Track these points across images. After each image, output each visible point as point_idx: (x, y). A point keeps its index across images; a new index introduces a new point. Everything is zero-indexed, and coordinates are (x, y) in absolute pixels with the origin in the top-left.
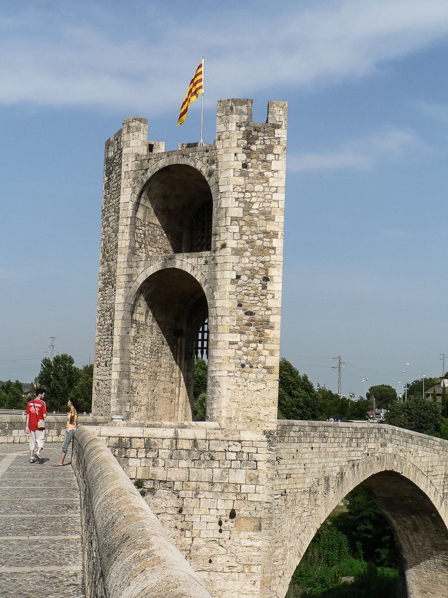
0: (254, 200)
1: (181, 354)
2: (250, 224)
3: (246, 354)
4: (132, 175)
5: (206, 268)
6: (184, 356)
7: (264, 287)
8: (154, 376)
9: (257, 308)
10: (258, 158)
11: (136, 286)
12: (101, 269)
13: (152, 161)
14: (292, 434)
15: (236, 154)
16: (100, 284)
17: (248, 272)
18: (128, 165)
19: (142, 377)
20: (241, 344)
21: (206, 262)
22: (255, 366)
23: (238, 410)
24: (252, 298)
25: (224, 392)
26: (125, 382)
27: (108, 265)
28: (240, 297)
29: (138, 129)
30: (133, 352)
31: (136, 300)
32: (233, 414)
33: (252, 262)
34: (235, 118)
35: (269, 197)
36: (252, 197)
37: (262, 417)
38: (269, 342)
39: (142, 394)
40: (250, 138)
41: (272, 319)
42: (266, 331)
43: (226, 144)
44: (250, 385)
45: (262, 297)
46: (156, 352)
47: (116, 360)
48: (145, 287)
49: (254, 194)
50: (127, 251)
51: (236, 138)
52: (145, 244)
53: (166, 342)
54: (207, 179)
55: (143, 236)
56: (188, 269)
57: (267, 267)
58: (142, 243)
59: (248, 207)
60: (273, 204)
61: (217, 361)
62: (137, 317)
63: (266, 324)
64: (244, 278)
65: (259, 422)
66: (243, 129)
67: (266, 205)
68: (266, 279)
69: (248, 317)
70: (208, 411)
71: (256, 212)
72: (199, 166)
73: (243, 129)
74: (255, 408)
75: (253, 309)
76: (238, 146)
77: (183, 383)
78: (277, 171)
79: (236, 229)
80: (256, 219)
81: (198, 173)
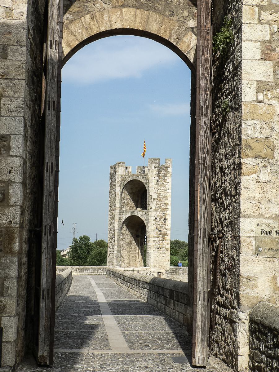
0: (161, 192)
1: (139, 244)
2: (160, 201)
3: (159, 245)
4: (120, 182)
5: (145, 216)
6: (140, 244)
7: (165, 222)
8: (129, 252)
9: (163, 229)
10: (162, 178)
11: (122, 221)
12: (109, 213)
13: (127, 178)
14: (180, 272)
15: (154, 177)
16: (109, 219)
17: (159, 217)
18: (119, 179)
19: (125, 252)
20: (157, 241)
21: (145, 214)
22: (162, 248)
23: (156, 263)
24: (161, 226)
25: (152, 257)
26: (119, 254)
27: (112, 212)
28: (157, 225)
29: (122, 166)
30: (122, 244)
31: (122, 226)
32: (155, 264)
33: (160, 213)
34: (154, 165)
35: (166, 191)
36: (160, 192)
37: (165, 265)
38: (166, 240)
39: (125, 258)
40: (159, 171)
41: (168, 233)
42: (166, 236)
43: (151, 174)
44: (160, 255)
45: (164, 225)
46: (129, 243)
47: (116, 247)
48: (125, 221)
49: (161, 191)
50: (119, 209)
51: (154, 171)
52: (125, 206)
53: (133, 240)
54: (145, 185)
55: (124, 203)
56: (140, 216)
57: (165, 215)
58: (124, 206)
59: (159, 195)
60: (167, 194)
61: (149, 247)
62: (123, 231)
63: (166, 234)
64: (158, 219)
65: (164, 267)
66: (157, 168)
67: (165, 194)
68: (165, 219)
69: (159, 232)
70: (147, 264)
71: (162, 197)
72: (142, 181)
73: (157, 168)
74: (162, 262)
75: (161, 229)
76: (155, 174)
77: (140, 253)
78: (168, 183)
79: (155, 202)
80: (162, 199)
81: (142, 183)
